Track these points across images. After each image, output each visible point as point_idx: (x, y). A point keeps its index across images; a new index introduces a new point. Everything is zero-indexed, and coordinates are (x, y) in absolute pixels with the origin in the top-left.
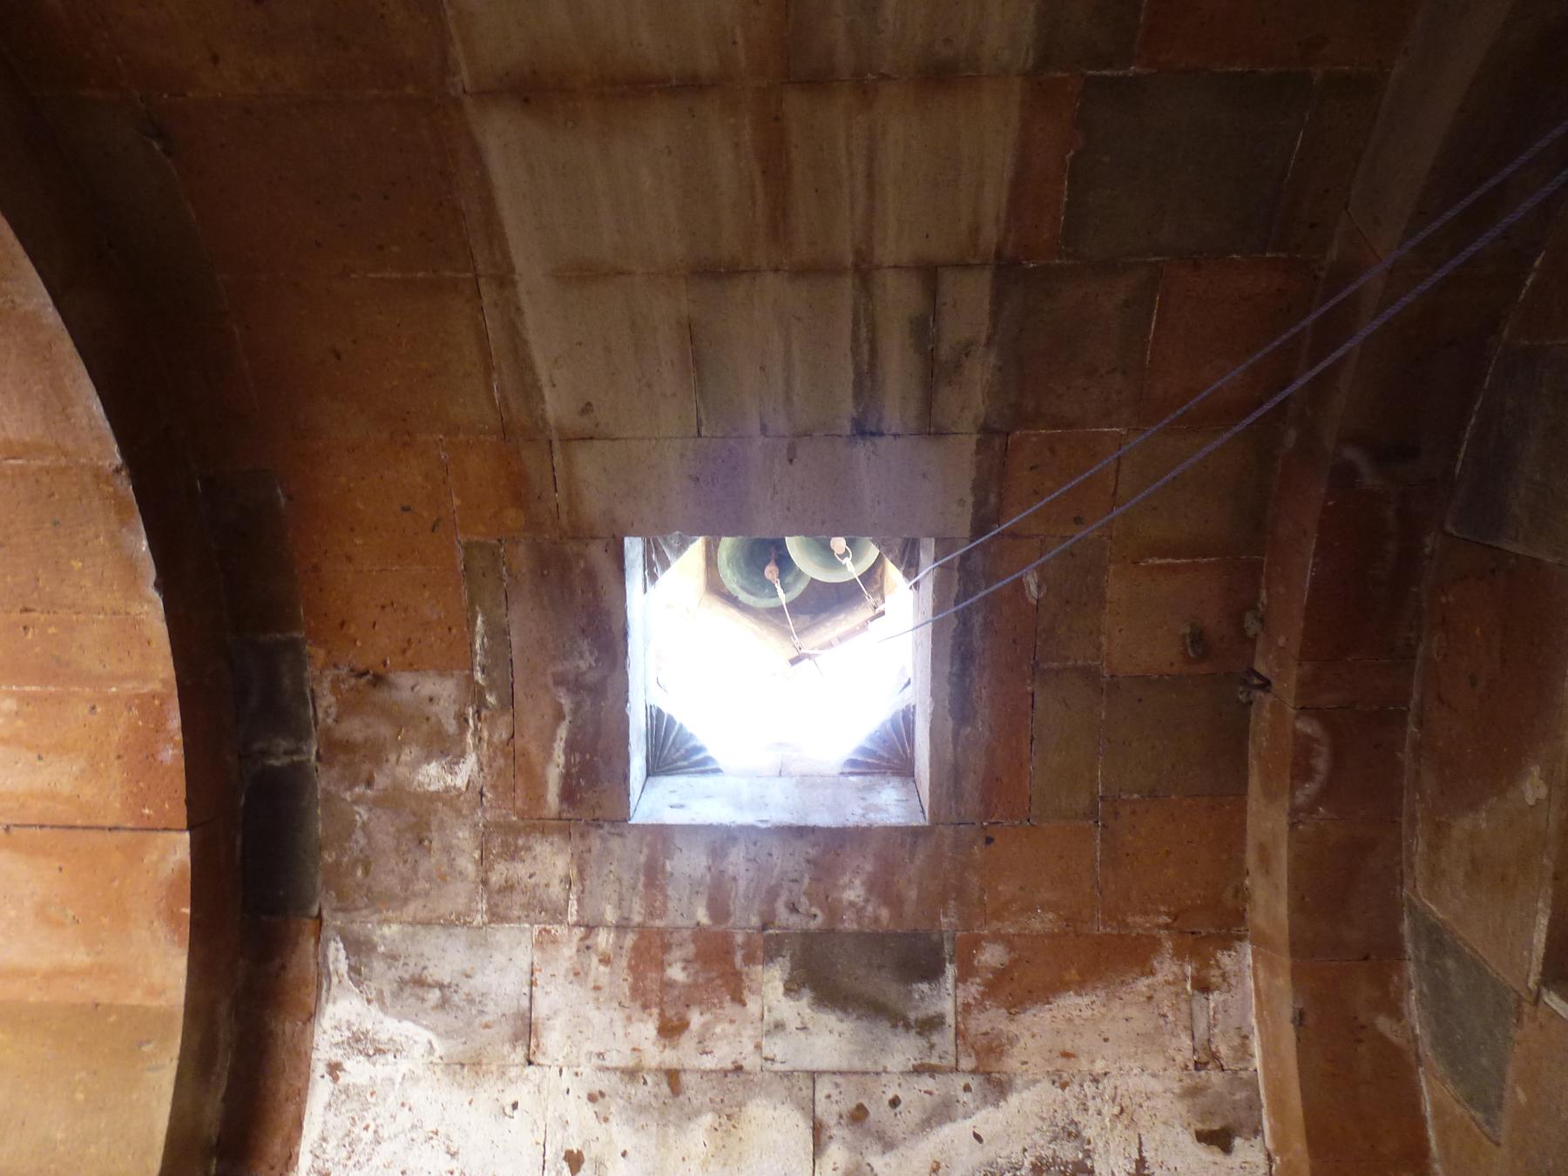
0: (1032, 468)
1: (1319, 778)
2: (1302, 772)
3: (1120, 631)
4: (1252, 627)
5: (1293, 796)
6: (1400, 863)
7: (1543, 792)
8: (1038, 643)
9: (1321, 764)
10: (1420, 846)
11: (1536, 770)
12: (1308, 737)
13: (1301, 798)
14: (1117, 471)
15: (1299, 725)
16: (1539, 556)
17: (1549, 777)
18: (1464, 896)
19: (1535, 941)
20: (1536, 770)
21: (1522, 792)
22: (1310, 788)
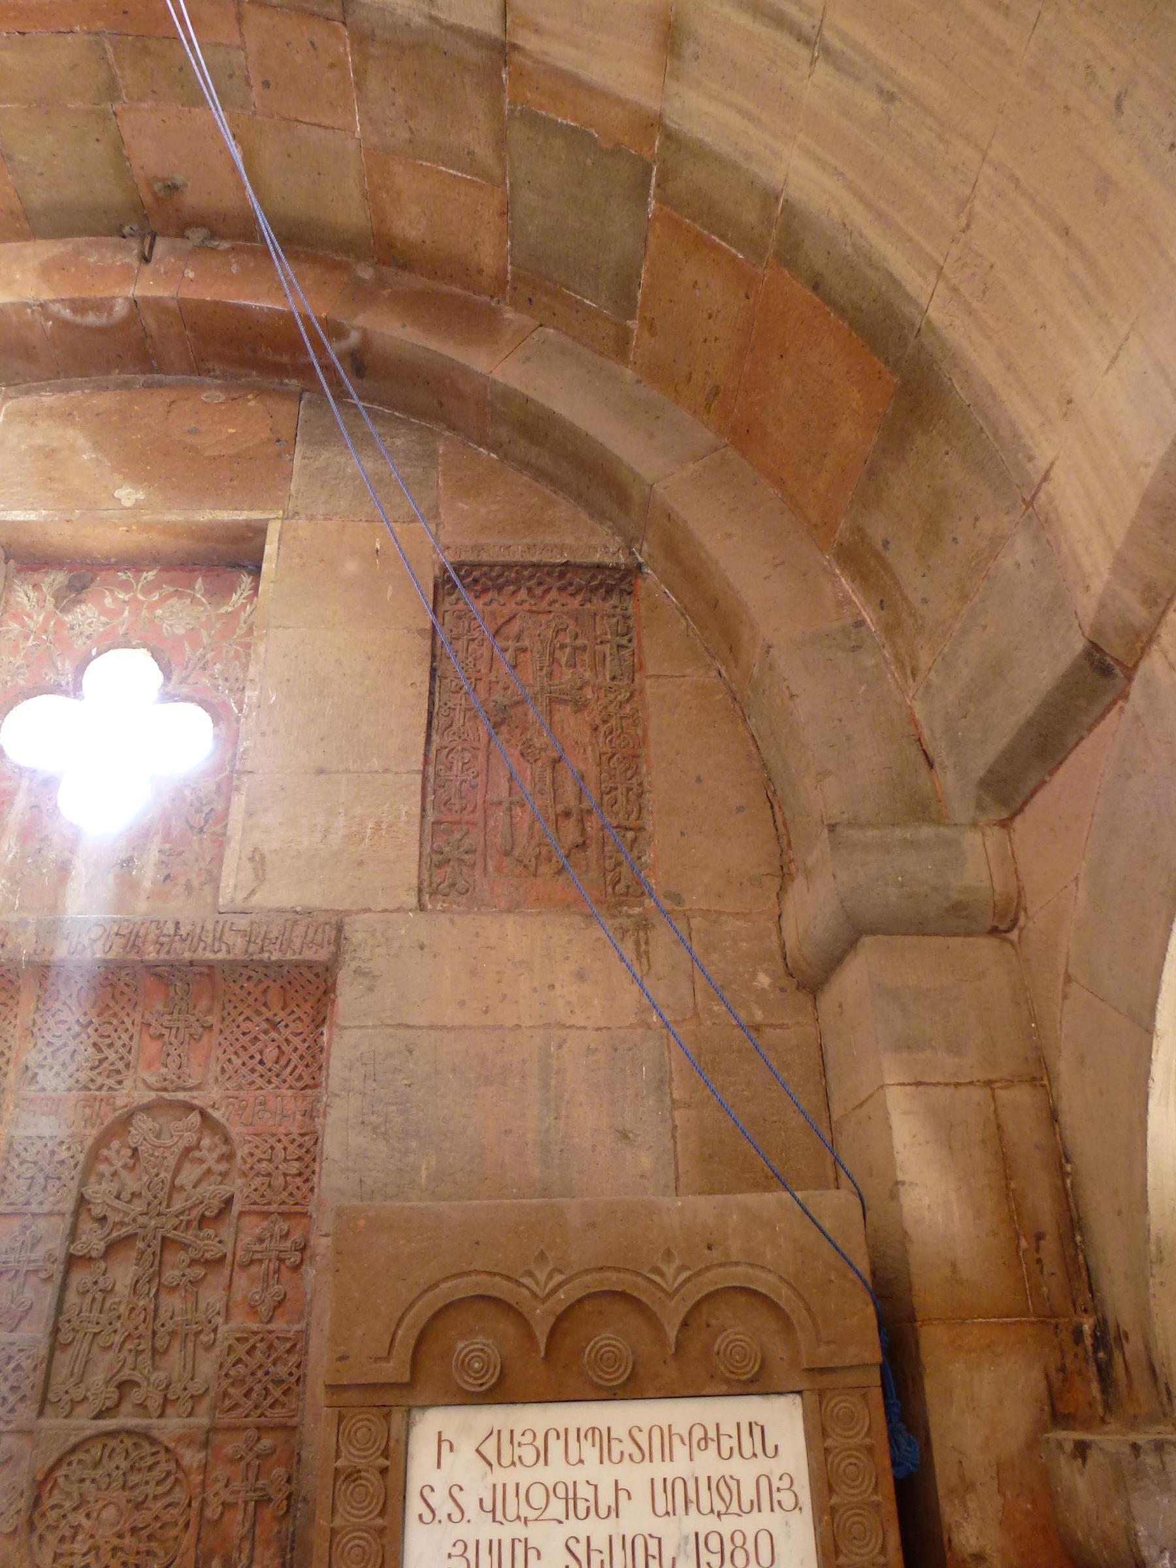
0: (312, 44)
1: (78, 319)
2: (79, 306)
3: (163, 121)
4: (196, 236)
5: (54, 301)
6: (26, 382)
7: (127, 503)
8: (130, 38)
9: (91, 319)
10: (48, 399)
11: (141, 495)
12: (112, 308)
13: (55, 308)
14: (319, 125)
15: (120, 301)
16: (295, 477)
17: (138, 506)
18: (23, 447)
19: (14, 512)
20: (141, 495)
21: (121, 487)
22: (67, 313)
